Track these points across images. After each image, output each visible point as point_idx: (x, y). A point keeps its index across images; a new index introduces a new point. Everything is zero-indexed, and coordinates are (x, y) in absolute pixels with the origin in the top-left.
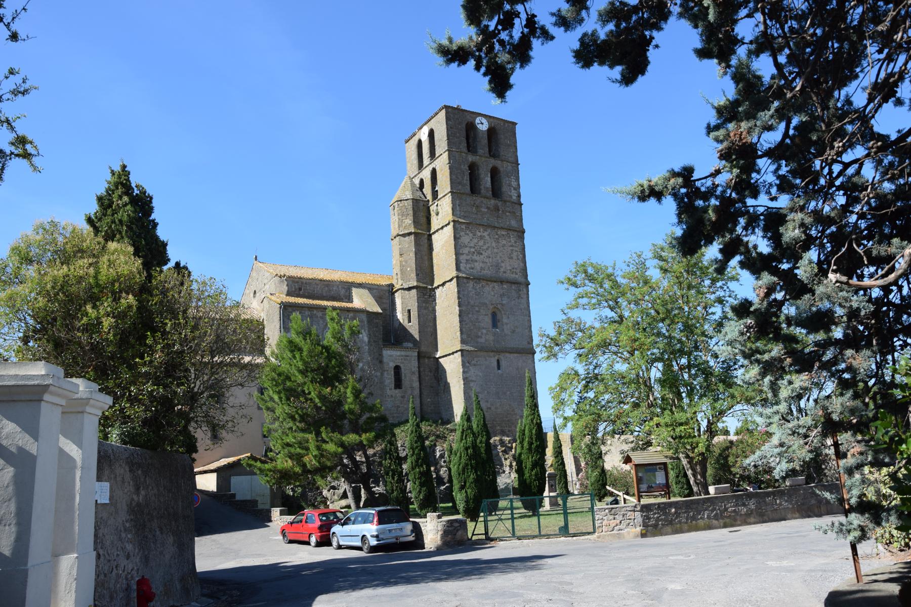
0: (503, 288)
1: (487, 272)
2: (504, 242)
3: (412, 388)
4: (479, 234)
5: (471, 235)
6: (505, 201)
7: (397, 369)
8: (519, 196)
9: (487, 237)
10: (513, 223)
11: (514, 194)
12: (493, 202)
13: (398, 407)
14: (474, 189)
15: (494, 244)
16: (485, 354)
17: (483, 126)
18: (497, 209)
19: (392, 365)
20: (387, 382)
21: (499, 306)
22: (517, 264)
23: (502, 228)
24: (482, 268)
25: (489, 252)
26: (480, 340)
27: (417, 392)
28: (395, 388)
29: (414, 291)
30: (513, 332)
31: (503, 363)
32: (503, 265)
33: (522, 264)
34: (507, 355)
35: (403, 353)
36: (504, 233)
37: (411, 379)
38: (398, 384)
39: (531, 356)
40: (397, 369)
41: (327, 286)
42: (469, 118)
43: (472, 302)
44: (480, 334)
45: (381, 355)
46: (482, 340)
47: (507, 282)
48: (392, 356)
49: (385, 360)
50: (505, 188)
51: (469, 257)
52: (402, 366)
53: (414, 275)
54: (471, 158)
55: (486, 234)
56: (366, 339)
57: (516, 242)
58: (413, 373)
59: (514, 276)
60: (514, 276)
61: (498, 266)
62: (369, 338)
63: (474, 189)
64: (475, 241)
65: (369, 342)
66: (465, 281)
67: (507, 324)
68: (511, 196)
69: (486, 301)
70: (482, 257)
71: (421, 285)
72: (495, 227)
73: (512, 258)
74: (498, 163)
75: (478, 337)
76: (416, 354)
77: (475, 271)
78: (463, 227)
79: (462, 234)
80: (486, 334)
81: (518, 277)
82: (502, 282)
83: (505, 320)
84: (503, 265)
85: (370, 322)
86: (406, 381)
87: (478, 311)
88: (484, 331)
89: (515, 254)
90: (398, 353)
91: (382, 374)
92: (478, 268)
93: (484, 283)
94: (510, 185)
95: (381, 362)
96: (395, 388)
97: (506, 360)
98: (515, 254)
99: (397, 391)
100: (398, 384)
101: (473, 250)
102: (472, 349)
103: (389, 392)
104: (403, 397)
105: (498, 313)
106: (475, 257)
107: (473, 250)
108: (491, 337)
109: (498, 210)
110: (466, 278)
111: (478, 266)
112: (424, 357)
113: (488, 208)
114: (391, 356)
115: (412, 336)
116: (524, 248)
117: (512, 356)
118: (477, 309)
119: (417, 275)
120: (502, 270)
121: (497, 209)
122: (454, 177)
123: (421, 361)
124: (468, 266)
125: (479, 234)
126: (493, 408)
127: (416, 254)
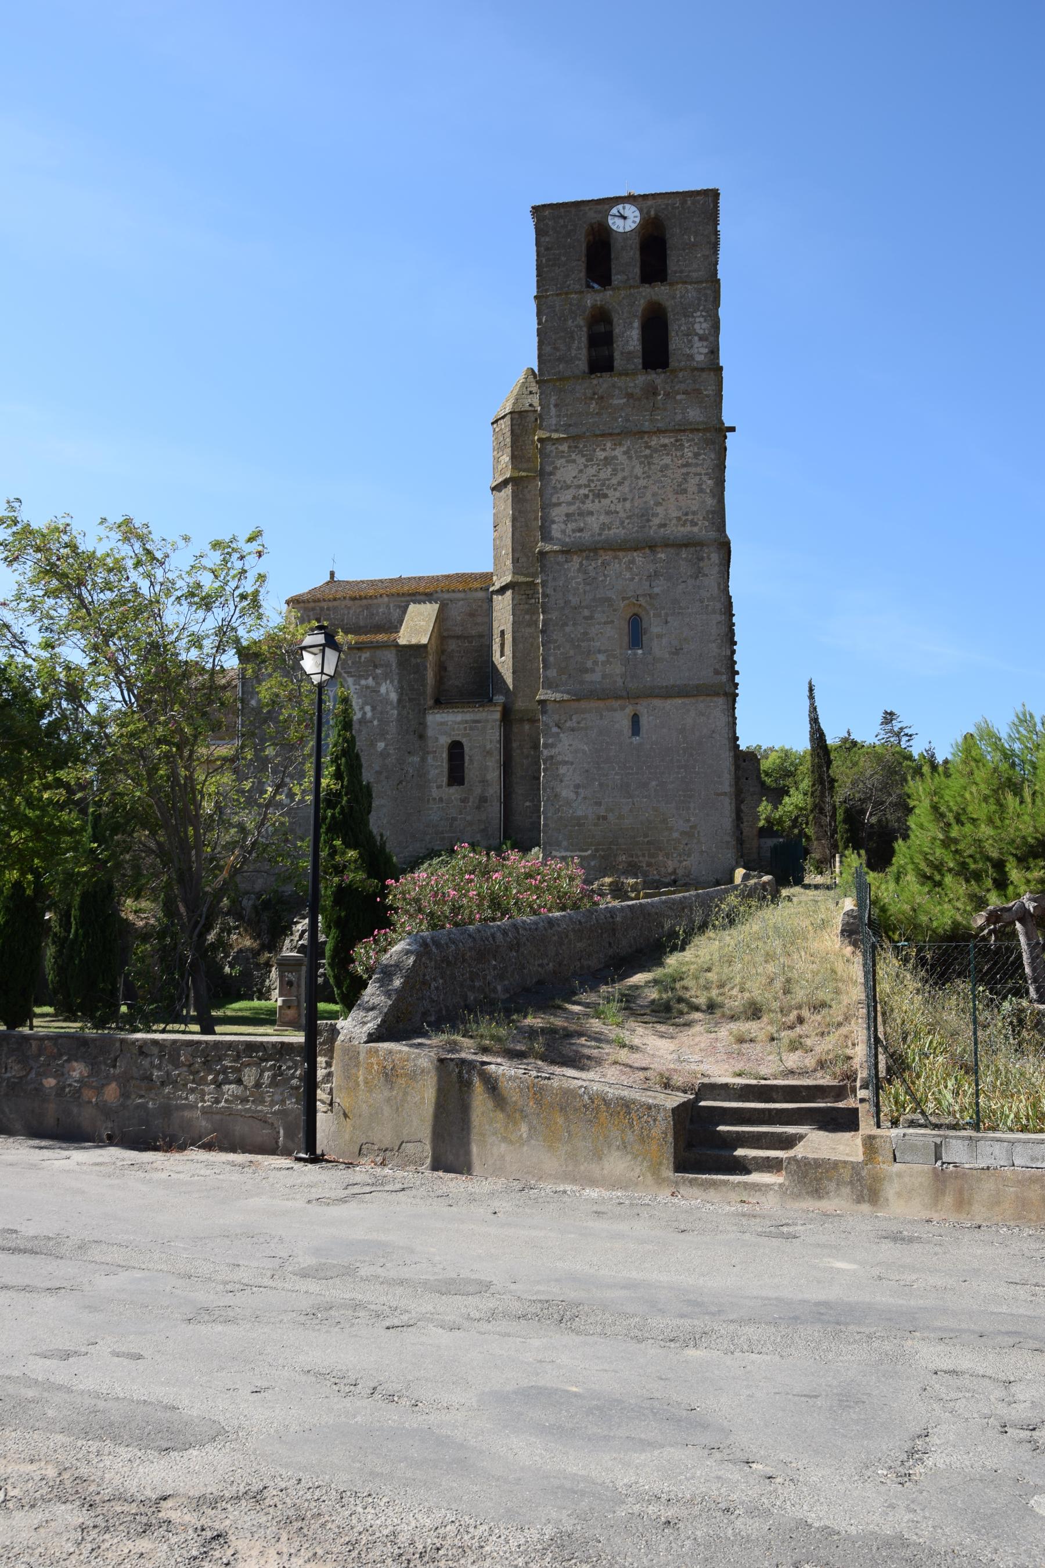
0: (654, 561)
1: (617, 532)
2: (667, 460)
3: (484, 782)
4: (601, 455)
5: (583, 460)
6: (674, 371)
7: (456, 750)
8: (714, 351)
9: (622, 458)
10: (694, 414)
11: (699, 352)
12: (641, 379)
13: (454, 819)
14: (601, 362)
15: (638, 470)
16: (600, 704)
17: (626, 221)
18: (652, 391)
19: (444, 741)
20: (433, 773)
21: (642, 601)
22: (697, 502)
23: (660, 431)
24: (603, 527)
25: (625, 488)
26: (588, 677)
27: (495, 790)
28: (450, 784)
29: (509, 593)
30: (677, 652)
31: (644, 721)
32: (659, 510)
33: (710, 502)
34: (657, 702)
35: (468, 717)
36: (667, 441)
37: (485, 767)
38: (456, 775)
39: (721, 701)
40: (456, 750)
41: (368, 607)
42: (592, 216)
43: (574, 601)
44: (589, 664)
45: (423, 724)
46: (596, 677)
47: (667, 545)
48: (445, 724)
49: (430, 733)
50: (676, 343)
51: (572, 509)
52: (464, 741)
53: (509, 562)
54: (591, 300)
55: (618, 452)
56: (394, 696)
57: (696, 455)
58: (489, 753)
59: (688, 528)
60: (688, 528)
61: (645, 515)
62: (401, 695)
63: (601, 362)
64: (591, 471)
65: (399, 701)
66: (561, 558)
67: (660, 636)
68: (691, 357)
69: (610, 594)
70: (606, 502)
71: (522, 579)
72: (641, 433)
73: (685, 491)
74: (659, 292)
75: (586, 671)
76: (497, 716)
77: (586, 535)
78: (564, 447)
79: (559, 462)
80: (608, 662)
81: (701, 530)
82: (652, 546)
83: (655, 630)
84: (659, 510)
85: (401, 664)
86: (471, 771)
87: (591, 618)
88: (601, 658)
89: (693, 481)
90: (459, 718)
91: (423, 760)
92: (596, 528)
93: (607, 556)
94: (690, 333)
95: (422, 737)
96: (450, 784)
97: (650, 713)
98: (693, 481)
99: (453, 790)
100: (456, 775)
101: (582, 491)
102: (566, 697)
103: (435, 793)
104: (464, 800)
105: (643, 614)
106: (589, 506)
107: (582, 491)
108: (617, 669)
109: (655, 394)
110: (562, 552)
111: (594, 523)
112: (521, 720)
113: (630, 396)
114: (442, 724)
115: (505, 683)
116: (721, 467)
117: (669, 704)
118: (586, 612)
119: (515, 560)
120: (656, 521)
121: (652, 391)
122: (548, 349)
123: (516, 728)
124: (571, 526)
125: (601, 455)
126: (611, 817)
127: (514, 519)
